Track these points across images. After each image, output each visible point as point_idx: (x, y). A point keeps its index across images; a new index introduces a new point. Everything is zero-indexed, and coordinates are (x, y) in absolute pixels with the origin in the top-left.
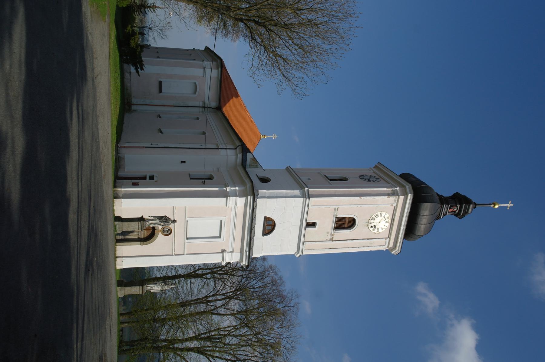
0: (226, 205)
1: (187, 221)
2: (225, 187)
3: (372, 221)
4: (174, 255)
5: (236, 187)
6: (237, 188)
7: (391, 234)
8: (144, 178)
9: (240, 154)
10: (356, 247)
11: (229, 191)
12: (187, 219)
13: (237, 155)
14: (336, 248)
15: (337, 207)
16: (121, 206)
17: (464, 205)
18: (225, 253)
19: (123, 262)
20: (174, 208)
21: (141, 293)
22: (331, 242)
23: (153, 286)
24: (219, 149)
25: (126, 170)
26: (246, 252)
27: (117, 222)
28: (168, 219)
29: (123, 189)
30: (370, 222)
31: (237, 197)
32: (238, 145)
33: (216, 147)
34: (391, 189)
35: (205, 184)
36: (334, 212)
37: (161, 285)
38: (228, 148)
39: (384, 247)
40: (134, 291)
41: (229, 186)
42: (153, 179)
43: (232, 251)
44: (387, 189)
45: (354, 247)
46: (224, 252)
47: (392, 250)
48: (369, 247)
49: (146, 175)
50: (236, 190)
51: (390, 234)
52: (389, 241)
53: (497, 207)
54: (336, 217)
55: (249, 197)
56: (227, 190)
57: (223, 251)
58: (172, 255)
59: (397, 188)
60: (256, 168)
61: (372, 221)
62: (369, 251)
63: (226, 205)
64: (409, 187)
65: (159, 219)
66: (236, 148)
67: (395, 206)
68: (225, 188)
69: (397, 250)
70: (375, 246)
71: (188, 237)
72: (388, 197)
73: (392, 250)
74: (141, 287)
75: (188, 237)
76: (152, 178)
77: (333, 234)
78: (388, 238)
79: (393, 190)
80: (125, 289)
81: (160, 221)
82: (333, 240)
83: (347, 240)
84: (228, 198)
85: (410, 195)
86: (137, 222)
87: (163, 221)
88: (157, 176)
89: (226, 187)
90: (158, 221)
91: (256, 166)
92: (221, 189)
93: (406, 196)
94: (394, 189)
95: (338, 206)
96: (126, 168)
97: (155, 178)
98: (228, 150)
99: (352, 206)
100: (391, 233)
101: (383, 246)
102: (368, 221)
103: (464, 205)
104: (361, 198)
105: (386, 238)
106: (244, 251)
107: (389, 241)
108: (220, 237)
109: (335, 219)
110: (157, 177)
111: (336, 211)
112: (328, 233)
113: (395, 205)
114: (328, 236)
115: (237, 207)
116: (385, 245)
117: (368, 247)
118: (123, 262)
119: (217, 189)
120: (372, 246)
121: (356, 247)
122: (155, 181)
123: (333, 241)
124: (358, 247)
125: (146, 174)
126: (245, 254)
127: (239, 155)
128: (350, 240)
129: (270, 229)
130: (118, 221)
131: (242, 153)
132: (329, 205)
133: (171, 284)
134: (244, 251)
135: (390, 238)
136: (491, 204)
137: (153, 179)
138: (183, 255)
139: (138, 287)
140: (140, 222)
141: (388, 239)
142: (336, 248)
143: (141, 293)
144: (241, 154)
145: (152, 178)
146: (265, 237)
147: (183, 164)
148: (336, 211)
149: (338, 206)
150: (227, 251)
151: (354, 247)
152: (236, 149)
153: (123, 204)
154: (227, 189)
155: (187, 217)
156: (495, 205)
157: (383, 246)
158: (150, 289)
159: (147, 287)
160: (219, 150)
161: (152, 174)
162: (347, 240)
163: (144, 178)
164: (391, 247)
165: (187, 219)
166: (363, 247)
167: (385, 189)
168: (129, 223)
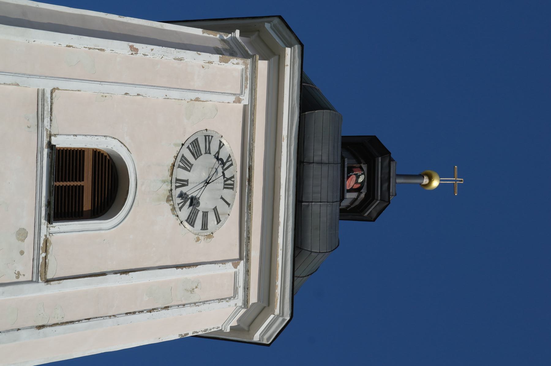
3: (181, 174)
7: (249, 238)
10: (139, 312)
14: (62, 324)
15: (47, 85)
17: (380, 159)
22: (42, 285)
30: (177, 180)
34: (218, 36)
36: (40, 118)
39: (232, 302)
44: (206, 35)
45: (134, 313)
47: (250, 325)
48: (188, 309)
51: (244, 241)
52: (247, 272)
53: (435, 183)
54: (51, 146)
59: (234, 31)
61: (181, 174)
62: (175, 336)
64: (271, 27)
67: (245, 106)
69: (277, 311)
70: (204, 302)
72: (221, 61)
73: (250, 325)
77: (46, 241)
78: (241, 258)
79: (223, 40)
82: (49, 277)
83: (103, 274)
85: (288, 50)
93: (274, 59)
94: (225, 38)
95: (53, 84)
99: (106, 88)
100: (249, 232)
101: (230, 298)
102: (168, 174)
103: (380, 159)
104: (136, 50)
105: (235, 262)
107: (247, 272)
109: (46, 151)
111: (47, 108)
112: (22, 234)
113: (246, 100)
114: (22, 253)
116: (234, 297)
117: (184, 305)
120: (195, 303)
121: (139, 312)
123: (48, 281)
124: (150, 311)
128: (115, 272)
132: (16, 74)
135: (248, 260)
136: (421, 176)
141: (242, 263)
142: (62, 324)
148: (47, 108)
149: (53, 84)
151: (134, 313)
156: (431, 179)
157: (230, 298)
162: (103, 274)
164: (253, 304)
166: (167, 308)
167: (198, 32)
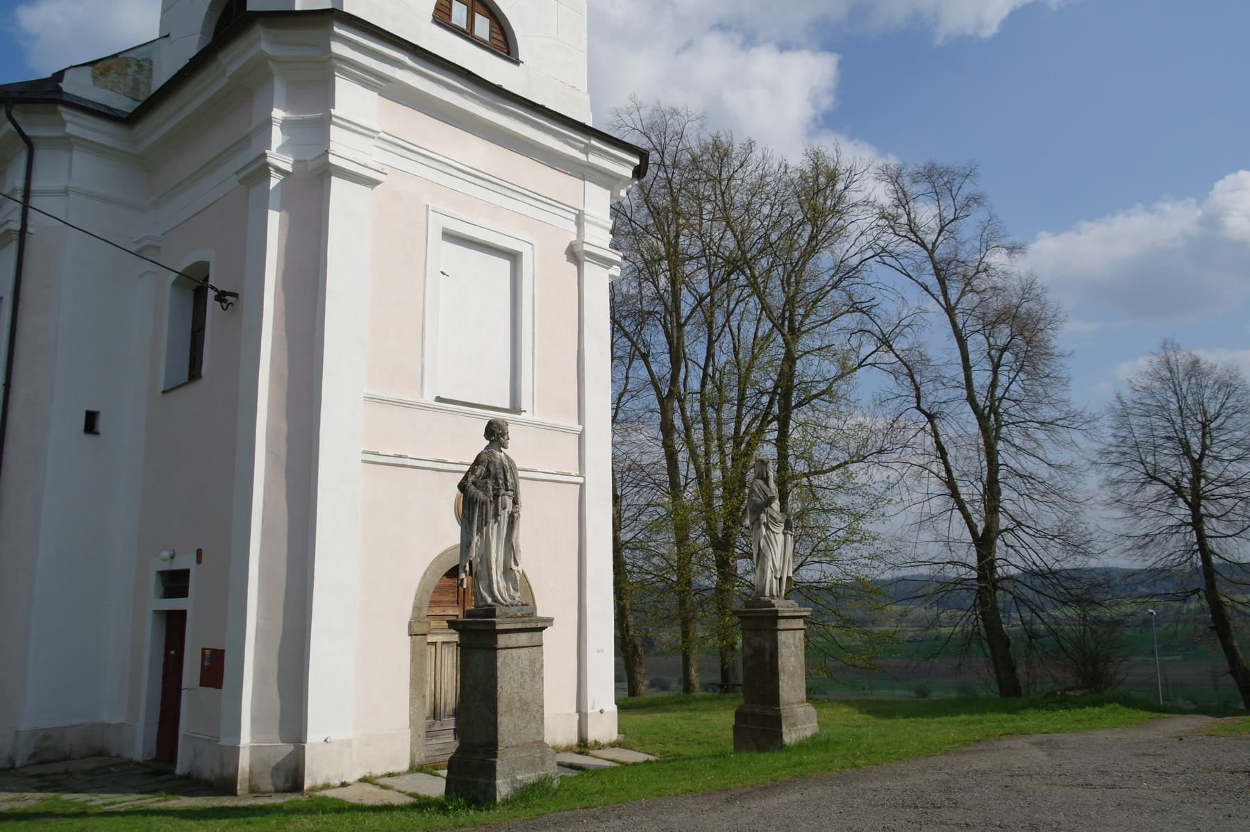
0: (372, 183)
1: (439, 399)
2: (268, 175)
4: (581, 480)
5: (269, 122)
6: (278, 114)
8: (174, 624)
9: (64, 124)
11: (291, 160)
12: (429, 399)
13: (68, 143)
16: (348, 743)
18: (586, 248)
19: (601, 712)
20: (373, 460)
21: (800, 624)
23: (770, 564)
24: (23, 232)
25: (121, 718)
26: (587, 149)
27: (499, 782)
28: (481, 470)
29: (246, 739)
31: (330, 115)
32: (10, 125)
33: (13, 248)
35: (235, 295)
37: (768, 528)
38: (20, 183)
40: (793, 659)
41: (265, 155)
42: (184, 574)
43: (573, 217)
46: (577, 249)
49: (155, 612)
50: (285, 125)
55: (337, 48)
56: (289, 168)
57: (575, 255)
58: (582, 486)
60: (151, 70)
63: (372, 183)
65: (484, 522)
66: (23, 144)
68: (274, 181)
71: (507, 406)
74: (782, 624)
75: (507, 406)
76: (175, 582)
80: (789, 704)
81: (496, 515)
84: (332, 160)
86: (501, 655)
87: (496, 496)
88: (165, 554)
89: (262, 170)
90: (493, 529)
91: (140, 66)
92: (273, 200)
96: (106, 718)
97: (178, 565)
98: (36, 185)
106: (582, 157)
108: (514, 257)
110: (172, 557)
115: (382, 135)
118: (601, 712)
119: (274, 220)
122: (199, 561)
125: (149, 619)
126: (595, 160)
127: (70, 129)
129: (487, 21)
130: (495, 778)
131: (60, 108)
133: (761, 482)
134: (582, 157)
137: (184, 574)
138: (581, 437)
139: (782, 637)
140: (502, 640)
143: (800, 624)
144: (66, 117)
145: (175, 582)
146: (522, 54)
147: (102, 424)
150: (574, 238)
152: (30, 144)
153: (334, 737)
154: (278, 170)
155: (417, 399)
158: (781, 579)
159: (772, 595)
160: (30, 229)
161: (153, 582)
163: (174, 624)
165: (429, 399)
168: (501, 707)
